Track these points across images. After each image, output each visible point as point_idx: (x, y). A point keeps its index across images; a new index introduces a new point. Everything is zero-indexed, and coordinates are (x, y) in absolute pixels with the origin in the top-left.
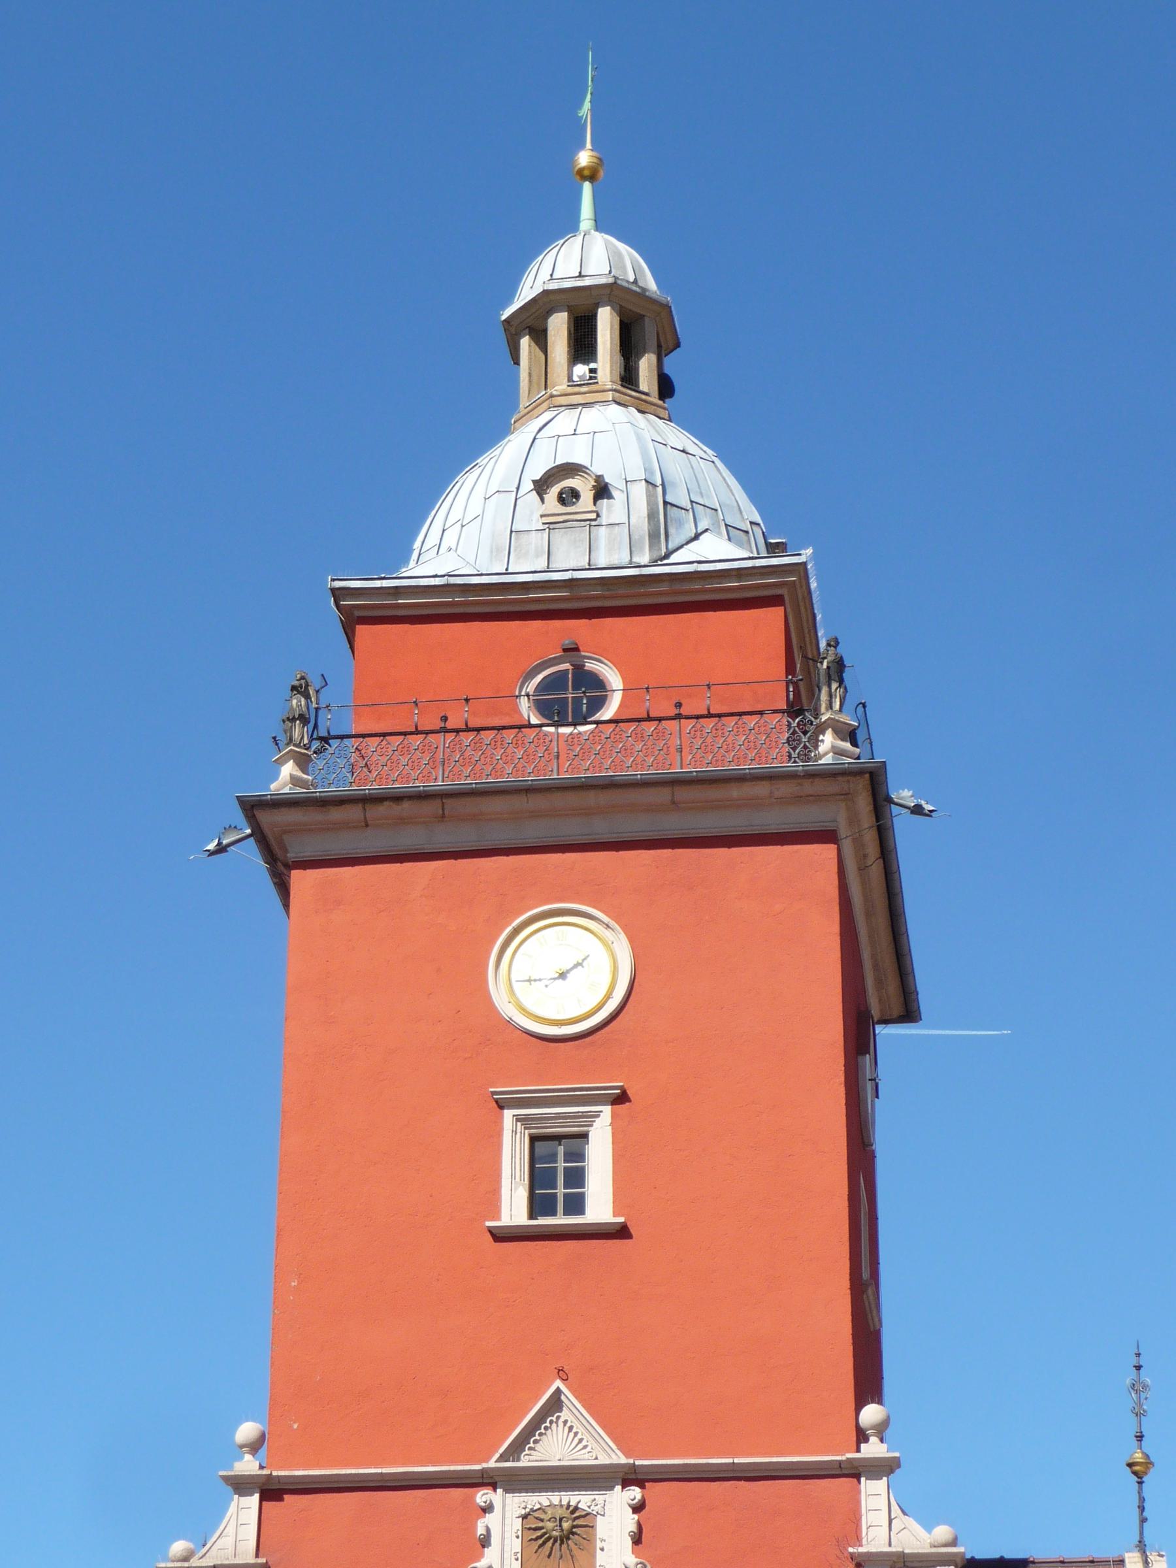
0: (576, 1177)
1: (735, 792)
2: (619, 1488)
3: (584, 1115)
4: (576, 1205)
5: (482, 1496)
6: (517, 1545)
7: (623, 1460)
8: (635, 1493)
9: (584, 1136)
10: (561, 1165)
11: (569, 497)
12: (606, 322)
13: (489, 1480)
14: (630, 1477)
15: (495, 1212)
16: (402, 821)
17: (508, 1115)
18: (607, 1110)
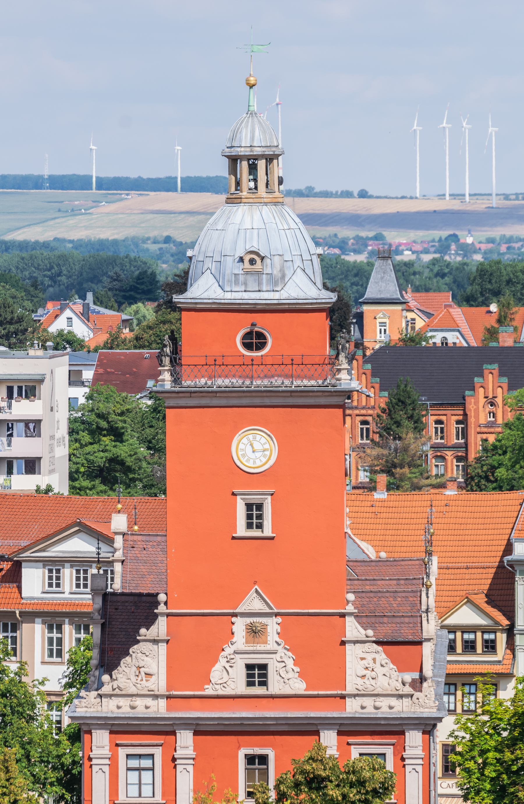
0: (260, 517)
1: (311, 394)
2: (274, 617)
3: (262, 499)
4: (260, 526)
5: (234, 619)
6: (244, 634)
7: (276, 611)
8: (279, 620)
9: (263, 503)
10: (255, 512)
11: (252, 262)
12: (261, 164)
13: (235, 615)
14: (277, 615)
15: (234, 528)
16: (202, 397)
17: (238, 497)
18: (269, 497)
